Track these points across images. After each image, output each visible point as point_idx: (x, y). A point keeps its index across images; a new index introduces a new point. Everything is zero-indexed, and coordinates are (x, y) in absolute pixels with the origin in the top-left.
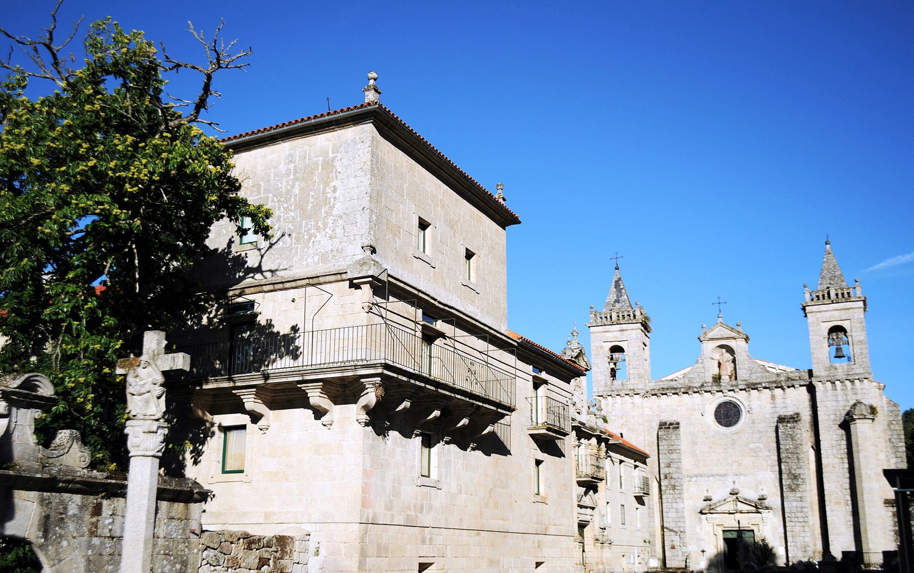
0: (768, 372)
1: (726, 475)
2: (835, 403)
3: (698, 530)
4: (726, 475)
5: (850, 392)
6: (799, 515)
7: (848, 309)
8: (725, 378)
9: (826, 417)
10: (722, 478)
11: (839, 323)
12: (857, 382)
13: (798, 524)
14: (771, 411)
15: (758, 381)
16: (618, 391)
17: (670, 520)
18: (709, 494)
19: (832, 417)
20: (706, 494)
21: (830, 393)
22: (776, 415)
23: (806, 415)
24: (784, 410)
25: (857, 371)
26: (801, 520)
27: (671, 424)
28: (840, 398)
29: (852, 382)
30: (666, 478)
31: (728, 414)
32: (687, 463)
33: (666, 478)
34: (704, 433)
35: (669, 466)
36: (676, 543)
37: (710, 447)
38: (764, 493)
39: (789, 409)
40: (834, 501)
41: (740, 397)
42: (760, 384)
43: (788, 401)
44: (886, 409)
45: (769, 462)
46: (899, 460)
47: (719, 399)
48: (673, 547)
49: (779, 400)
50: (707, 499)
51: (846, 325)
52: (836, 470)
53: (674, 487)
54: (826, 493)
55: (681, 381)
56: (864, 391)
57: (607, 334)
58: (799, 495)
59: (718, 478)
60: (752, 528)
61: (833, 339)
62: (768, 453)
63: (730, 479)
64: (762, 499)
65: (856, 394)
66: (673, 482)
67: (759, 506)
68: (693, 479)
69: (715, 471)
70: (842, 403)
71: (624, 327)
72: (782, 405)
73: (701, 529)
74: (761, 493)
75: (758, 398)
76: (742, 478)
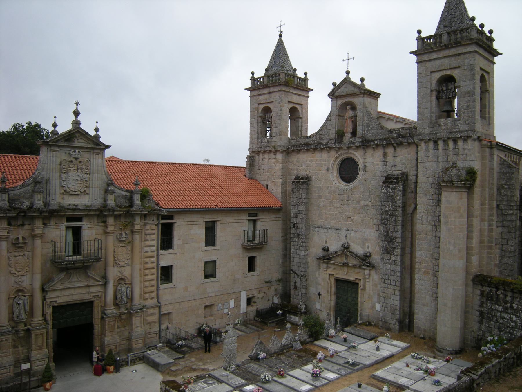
1: (340, 229)
2: (434, 165)
3: (317, 275)
4: (340, 229)
6: (392, 278)
7: (459, 55)
8: (347, 137)
9: (425, 180)
10: (338, 232)
11: (449, 72)
12: (460, 143)
13: (390, 286)
14: (381, 169)
16: (265, 147)
17: (294, 264)
18: (328, 245)
19: (431, 180)
21: (432, 152)
22: (385, 174)
24: (393, 168)
25: (461, 128)
26: (393, 283)
27: (302, 178)
28: (440, 159)
29: (455, 141)
31: (348, 171)
32: (315, 214)
33: (294, 227)
35: (296, 217)
36: (298, 285)
37: (331, 202)
38: (370, 250)
39: (398, 168)
40: (423, 270)
41: (358, 156)
42: (372, 141)
43: (398, 159)
45: (375, 221)
46: (505, 230)
48: (295, 288)
49: (390, 159)
51: (455, 73)
52: (429, 238)
56: (466, 151)
57: (261, 97)
58: (393, 258)
59: (334, 231)
60: (357, 281)
61: (443, 91)
62: (374, 212)
63: (343, 233)
65: (457, 154)
66: (298, 230)
67: (365, 261)
68: (317, 230)
69: (333, 224)
70: (441, 165)
72: (392, 164)
73: (319, 275)
74: (367, 250)
75: (372, 155)
76: (353, 233)
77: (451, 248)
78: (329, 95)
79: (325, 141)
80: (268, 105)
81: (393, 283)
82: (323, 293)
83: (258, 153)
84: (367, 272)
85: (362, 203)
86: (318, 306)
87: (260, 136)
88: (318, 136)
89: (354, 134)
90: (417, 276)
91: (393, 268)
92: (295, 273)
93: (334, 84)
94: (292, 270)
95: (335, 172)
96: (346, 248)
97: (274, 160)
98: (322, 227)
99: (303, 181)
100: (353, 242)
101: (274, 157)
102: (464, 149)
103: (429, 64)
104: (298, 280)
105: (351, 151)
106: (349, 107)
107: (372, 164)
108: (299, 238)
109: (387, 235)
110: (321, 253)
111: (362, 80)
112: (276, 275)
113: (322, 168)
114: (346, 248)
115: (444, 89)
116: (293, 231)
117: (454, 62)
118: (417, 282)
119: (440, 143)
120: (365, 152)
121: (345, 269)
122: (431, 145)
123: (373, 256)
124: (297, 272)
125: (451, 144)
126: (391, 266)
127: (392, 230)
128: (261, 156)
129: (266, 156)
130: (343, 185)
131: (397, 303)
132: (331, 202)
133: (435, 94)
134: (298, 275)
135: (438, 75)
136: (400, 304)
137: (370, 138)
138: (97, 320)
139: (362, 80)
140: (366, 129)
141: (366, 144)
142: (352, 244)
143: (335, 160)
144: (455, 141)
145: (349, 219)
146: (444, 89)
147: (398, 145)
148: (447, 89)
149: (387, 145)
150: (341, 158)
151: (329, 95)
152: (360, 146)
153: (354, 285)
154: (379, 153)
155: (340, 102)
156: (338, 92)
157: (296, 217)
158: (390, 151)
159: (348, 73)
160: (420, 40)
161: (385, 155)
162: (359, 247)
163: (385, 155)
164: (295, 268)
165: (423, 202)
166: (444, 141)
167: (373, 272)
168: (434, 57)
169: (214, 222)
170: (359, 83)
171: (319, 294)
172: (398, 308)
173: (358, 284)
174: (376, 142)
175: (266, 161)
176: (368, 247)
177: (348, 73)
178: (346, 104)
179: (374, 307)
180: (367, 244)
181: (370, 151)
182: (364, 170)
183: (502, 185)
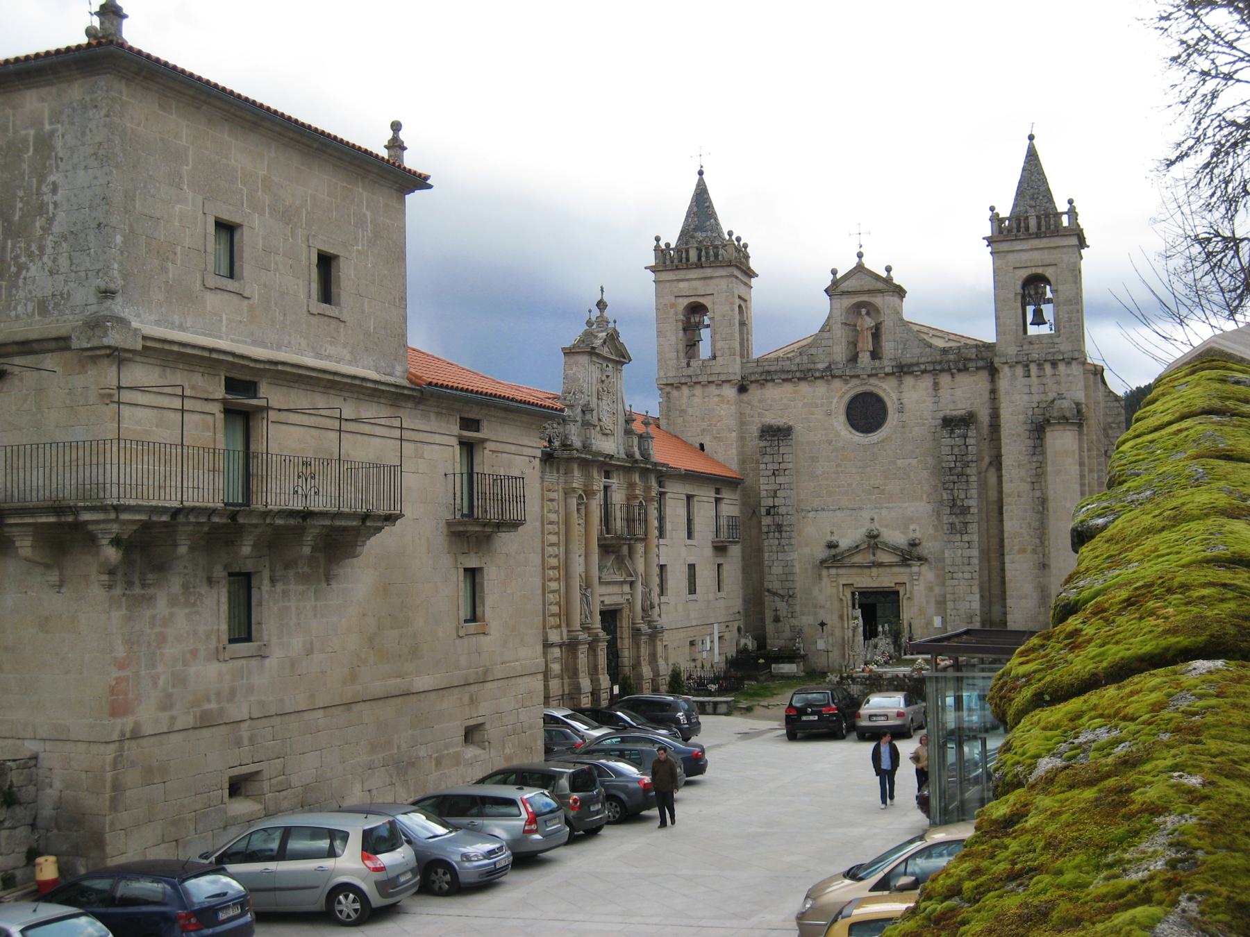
0: (930, 346)
2: (1025, 397)
3: (816, 592)
5: (1049, 381)
6: (966, 568)
8: (865, 358)
11: (1040, 271)
12: (1062, 367)
13: (963, 582)
15: (914, 360)
18: (834, 538)
19: (1022, 418)
20: (829, 538)
21: (1021, 381)
23: (984, 416)
29: (1054, 364)
30: (768, 513)
31: (866, 413)
33: (768, 513)
34: (830, 443)
37: (838, 465)
38: (918, 535)
39: (960, 406)
40: (1017, 548)
41: (886, 389)
42: (918, 364)
44: (1102, 404)
47: (855, 388)
48: (777, 619)
50: (832, 546)
51: (1049, 273)
52: (1023, 500)
53: (779, 528)
54: (1006, 535)
55: (798, 360)
57: (682, 285)
58: (966, 538)
59: (848, 512)
60: (897, 588)
61: (1030, 296)
63: (866, 515)
64: (913, 544)
65: (1058, 383)
67: (909, 555)
68: (811, 515)
70: (1036, 398)
71: (708, 272)
73: (821, 591)
74: (912, 535)
77: (1068, 505)
78: (826, 291)
79: (821, 366)
80: (701, 300)
81: (967, 576)
82: (832, 620)
83: (678, 386)
84: (915, 569)
85: (899, 462)
86: (821, 645)
87: (682, 355)
88: (805, 358)
89: (875, 355)
90: (1007, 559)
91: (967, 553)
92: (775, 594)
93: (834, 272)
94: (768, 591)
95: (842, 418)
96: (873, 536)
97: (716, 399)
98: (823, 510)
99: (776, 434)
100: (886, 526)
101: (717, 392)
102: (1068, 375)
103: (1011, 257)
104: (781, 605)
105: (873, 381)
106: (864, 311)
107: (914, 403)
108: (780, 532)
109: (954, 505)
110: (821, 553)
111: (888, 269)
112: (737, 604)
113: (817, 412)
114: (873, 536)
115: (1032, 292)
116: (766, 521)
117: (1046, 257)
118: (1008, 566)
119: (1033, 367)
120: (901, 382)
121: (874, 571)
122: (1019, 370)
123: (924, 544)
124: (780, 592)
125: (1048, 367)
126: (965, 553)
127: (963, 496)
128: (685, 390)
129: (698, 391)
130: (858, 437)
131: (976, 605)
132: (838, 465)
133: (1019, 297)
134: (783, 597)
135: (1024, 274)
136: (982, 605)
137: (909, 361)
138: (626, 642)
139: (888, 269)
140: (901, 346)
141: (902, 370)
142: (882, 530)
143: (841, 397)
144: (1054, 364)
145: (876, 491)
146: (1032, 292)
147: (959, 370)
148: (1037, 293)
149: (942, 371)
150: (852, 393)
151: (826, 291)
152: (893, 374)
153: (891, 597)
154: (927, 382)
155: (848, 302)
156: (844, 286)
157: (775, 496)
158: (945, 379)
159: (860, 255)
160: (996, 219)
161: (936, 386)
162: (897, 533)
163: (936, 386)
164: (776, 586)
165: (1014, 449)
166: (1039, 365)
167: (925, 568)
168: (1019, 248)
169: (693, 496)
170: (884, 274)
171: (822, 624)
172: (978, 612)
173: (898, 593)
174: (923, 367)
175: (697, 400)
176: (914, 531)
177: (860, 255)
178: (859, 306)
179: (929, 623)
180: (912, 527)
181: (909, 381)
182: (901, 411)
183: (1109, 424)
